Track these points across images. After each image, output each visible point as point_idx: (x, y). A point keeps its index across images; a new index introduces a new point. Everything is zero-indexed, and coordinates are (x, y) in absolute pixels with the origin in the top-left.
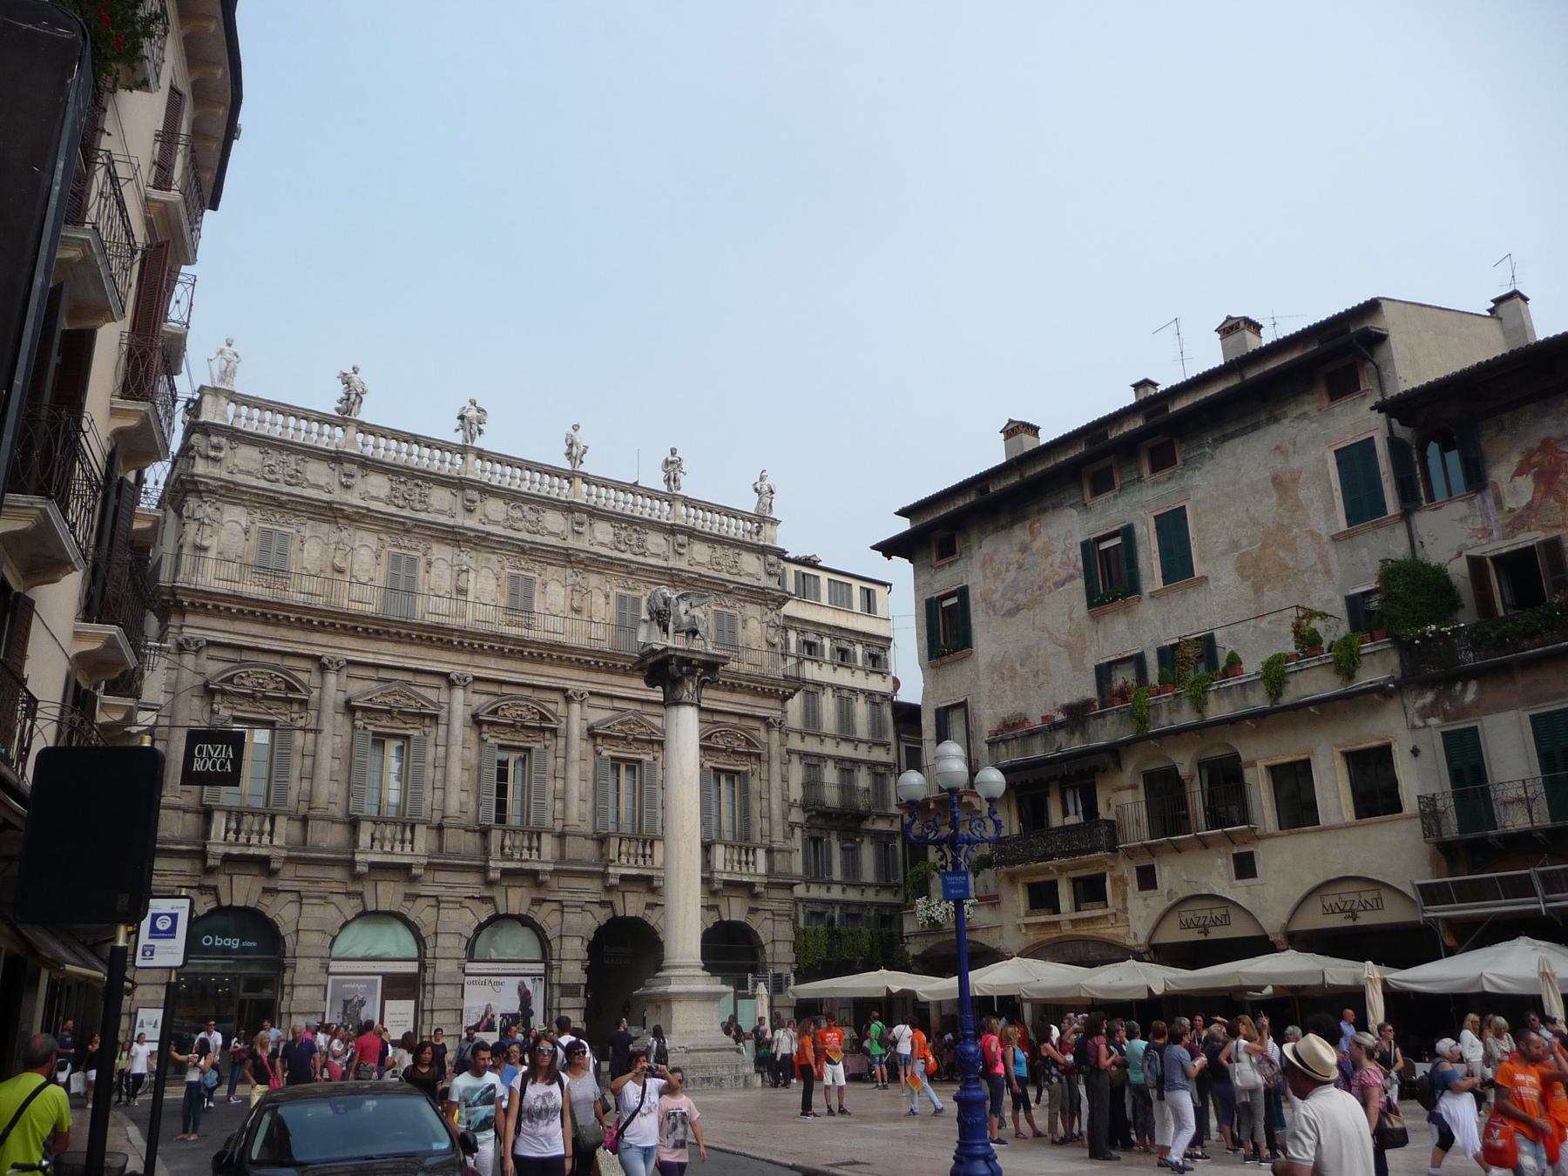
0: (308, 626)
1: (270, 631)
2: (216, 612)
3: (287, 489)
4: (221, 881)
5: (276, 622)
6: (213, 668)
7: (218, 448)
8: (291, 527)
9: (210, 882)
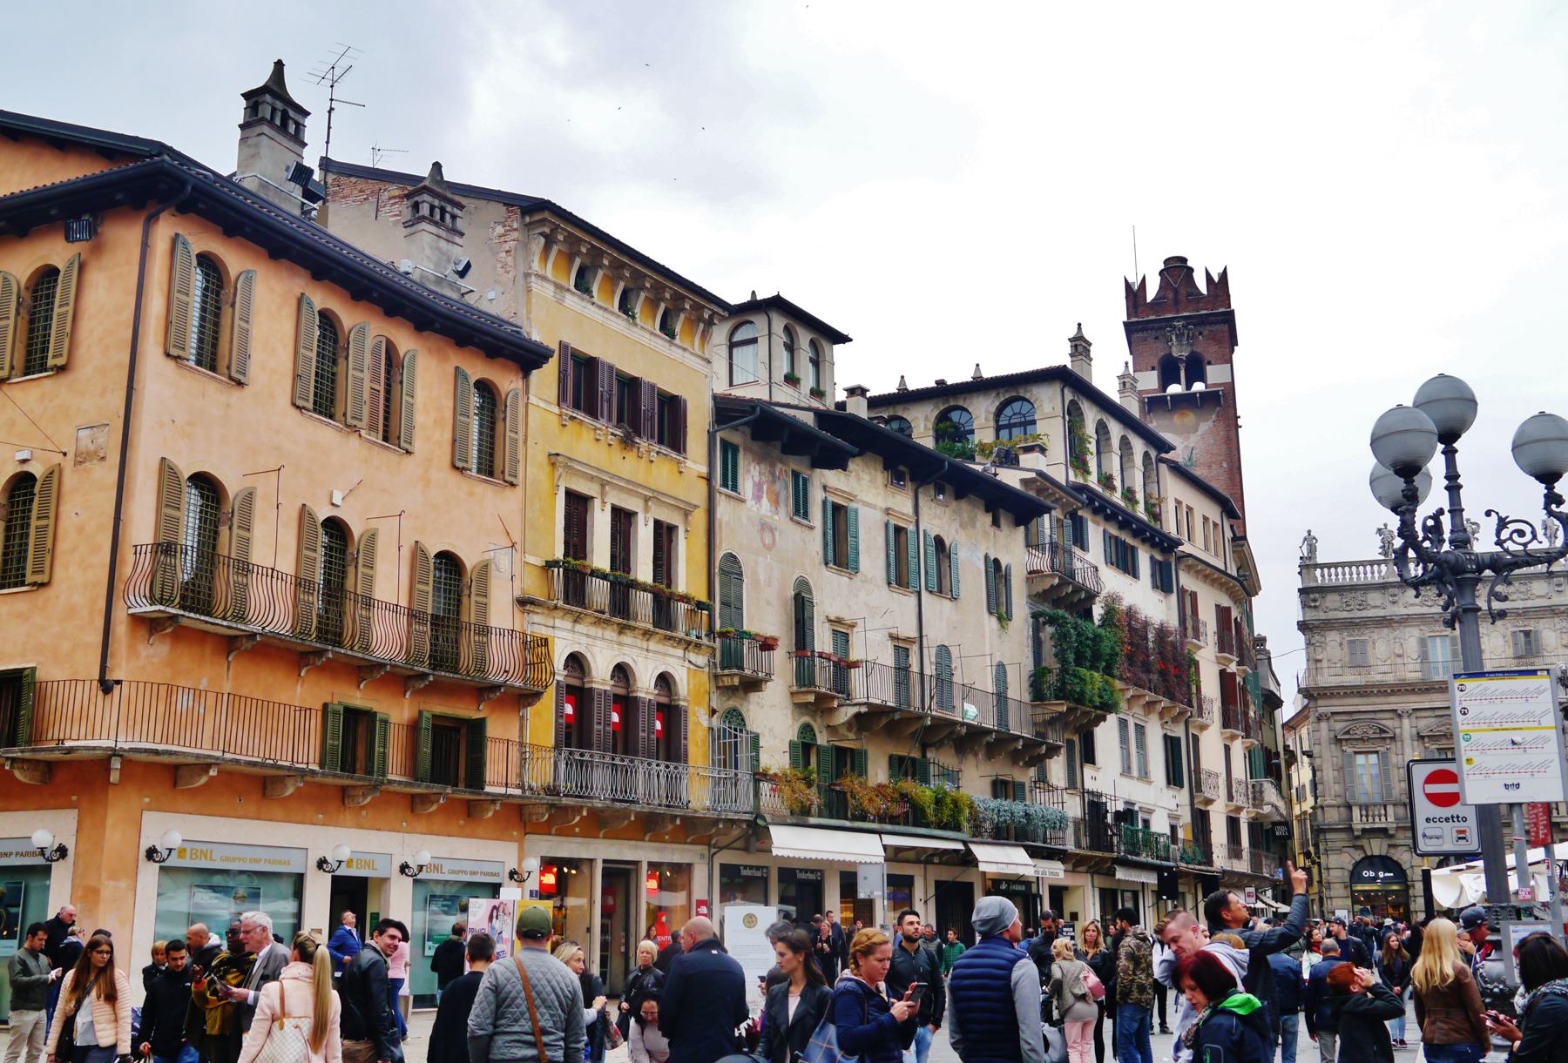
0: (1385, 694)
1: (1365, 700)
2: (1332, 696)
3: (1359, 614)
4: (1364, 842)
5: (1371, 694)
6: (1339, 726)
7: (1315, 600)
8: (1369, 635)
9: (1359, 843)
